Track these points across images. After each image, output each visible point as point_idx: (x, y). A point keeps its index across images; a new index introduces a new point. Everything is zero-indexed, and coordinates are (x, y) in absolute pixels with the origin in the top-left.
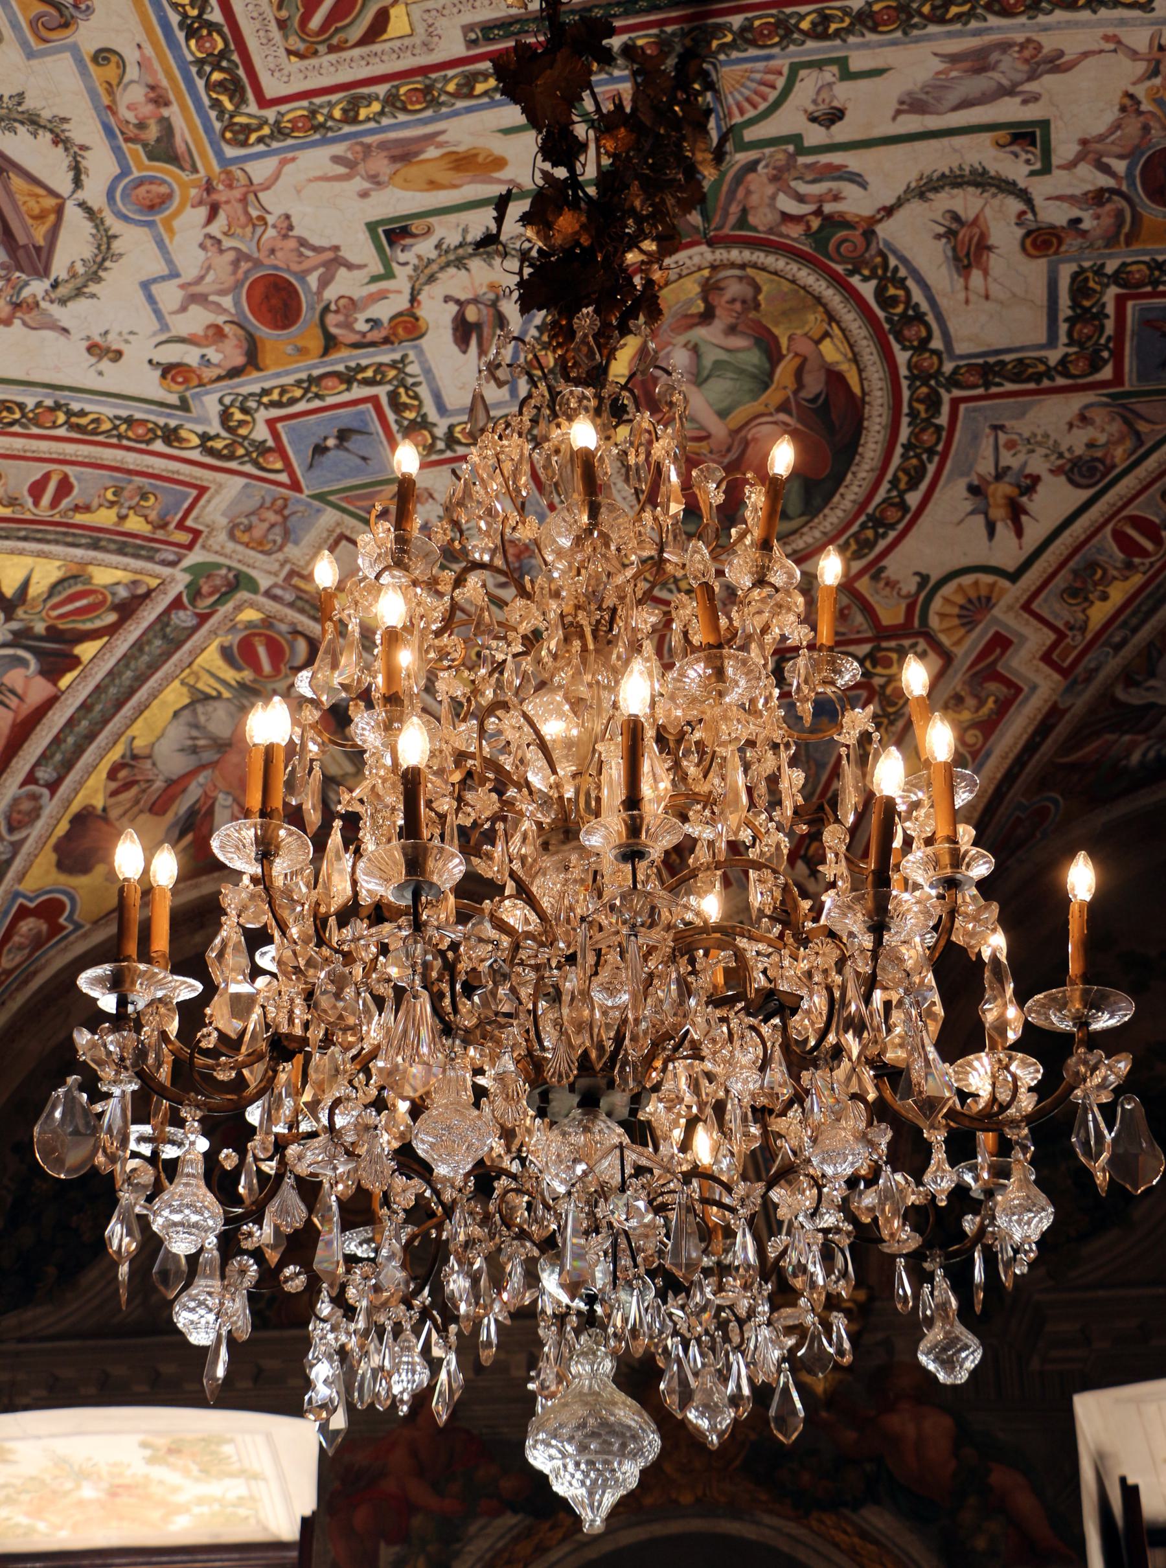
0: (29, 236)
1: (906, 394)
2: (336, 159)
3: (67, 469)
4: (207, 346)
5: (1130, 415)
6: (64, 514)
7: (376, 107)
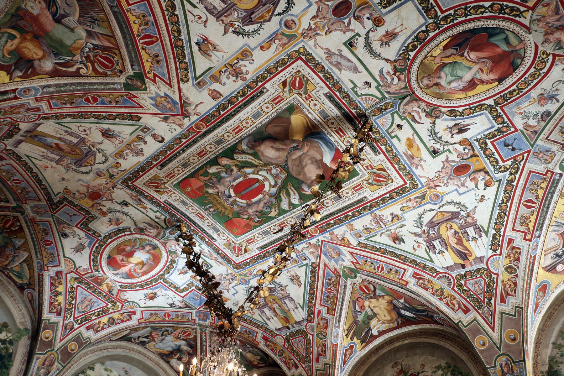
1: (445, 27)
2: (417, 168)
3: (523, 200)
6: (538, 201)
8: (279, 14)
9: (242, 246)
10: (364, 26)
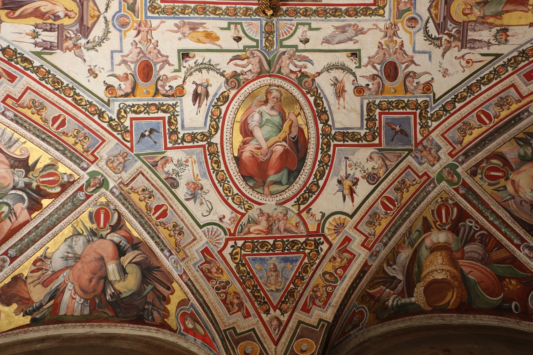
0: (87, 23)
1: (321, 140)
2: (176, 25)
4: (122, 81)
5: (383, 157)
7: (190, 10)
8: (427, 22)
10: (363, 77)
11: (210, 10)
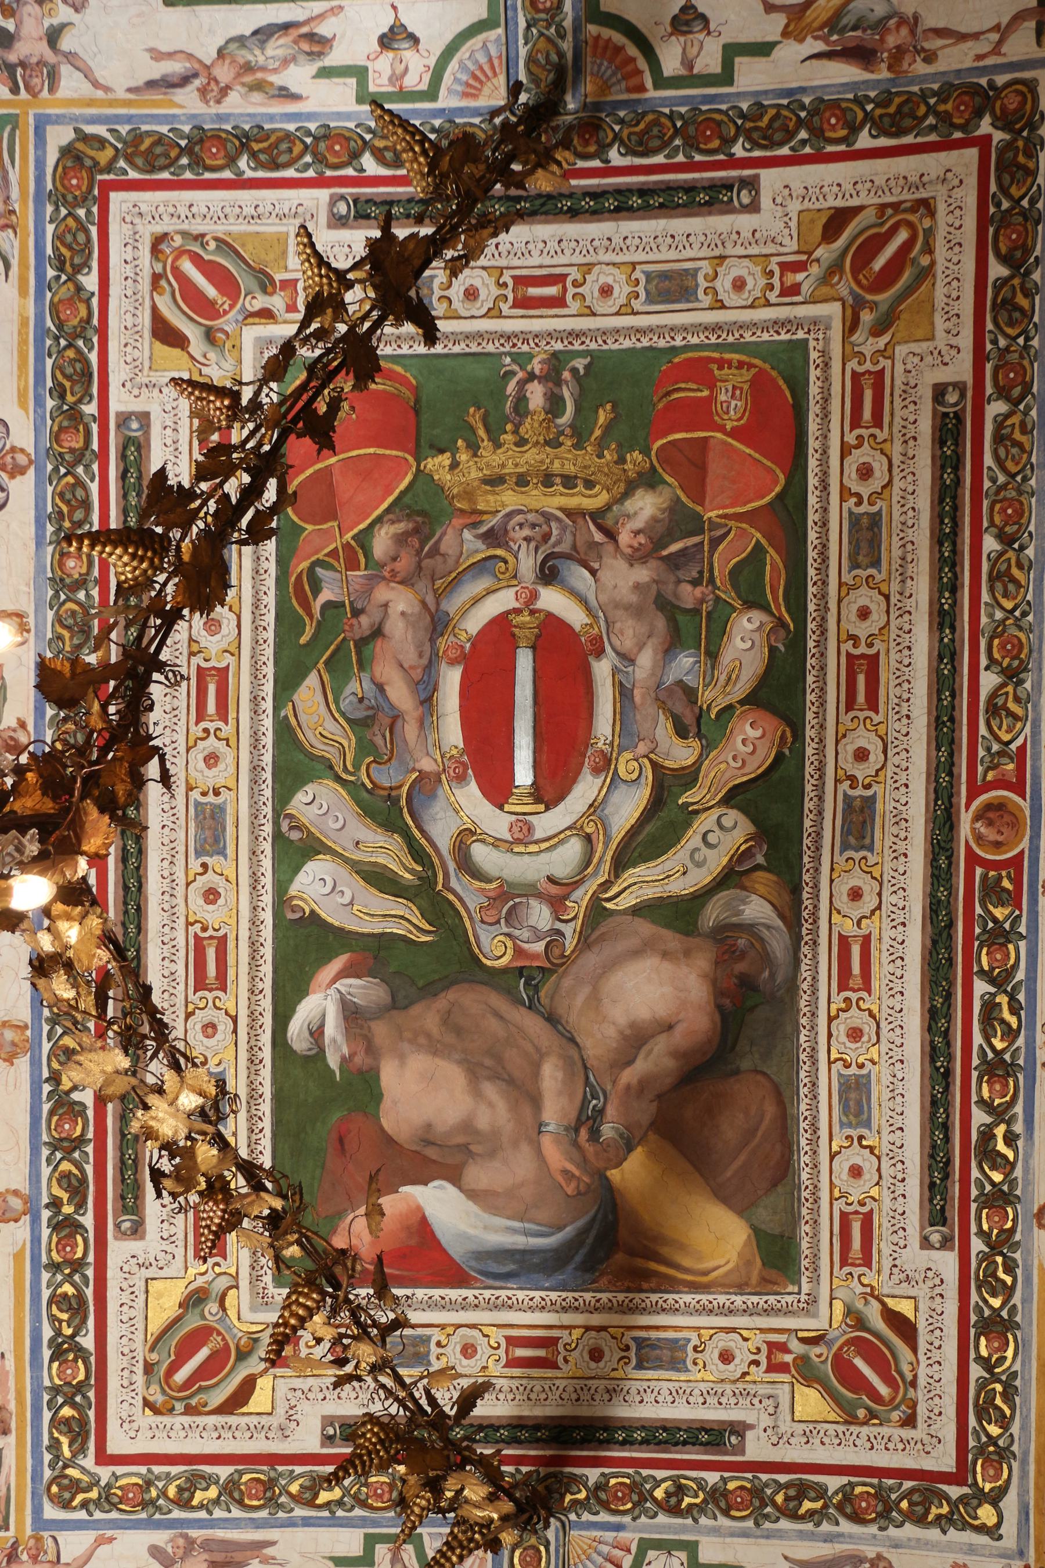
9: (210, 336)
11: (294, 1488)
